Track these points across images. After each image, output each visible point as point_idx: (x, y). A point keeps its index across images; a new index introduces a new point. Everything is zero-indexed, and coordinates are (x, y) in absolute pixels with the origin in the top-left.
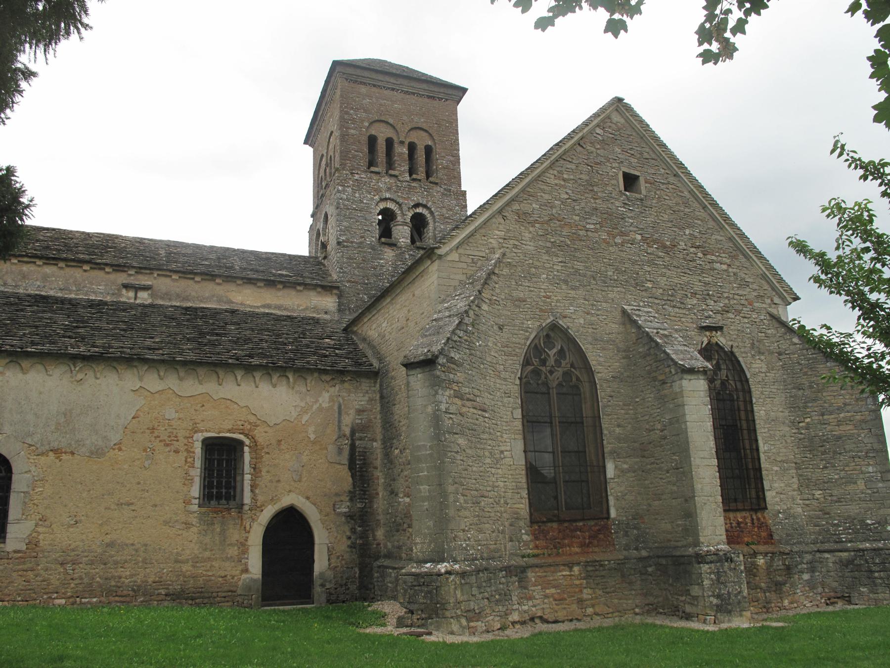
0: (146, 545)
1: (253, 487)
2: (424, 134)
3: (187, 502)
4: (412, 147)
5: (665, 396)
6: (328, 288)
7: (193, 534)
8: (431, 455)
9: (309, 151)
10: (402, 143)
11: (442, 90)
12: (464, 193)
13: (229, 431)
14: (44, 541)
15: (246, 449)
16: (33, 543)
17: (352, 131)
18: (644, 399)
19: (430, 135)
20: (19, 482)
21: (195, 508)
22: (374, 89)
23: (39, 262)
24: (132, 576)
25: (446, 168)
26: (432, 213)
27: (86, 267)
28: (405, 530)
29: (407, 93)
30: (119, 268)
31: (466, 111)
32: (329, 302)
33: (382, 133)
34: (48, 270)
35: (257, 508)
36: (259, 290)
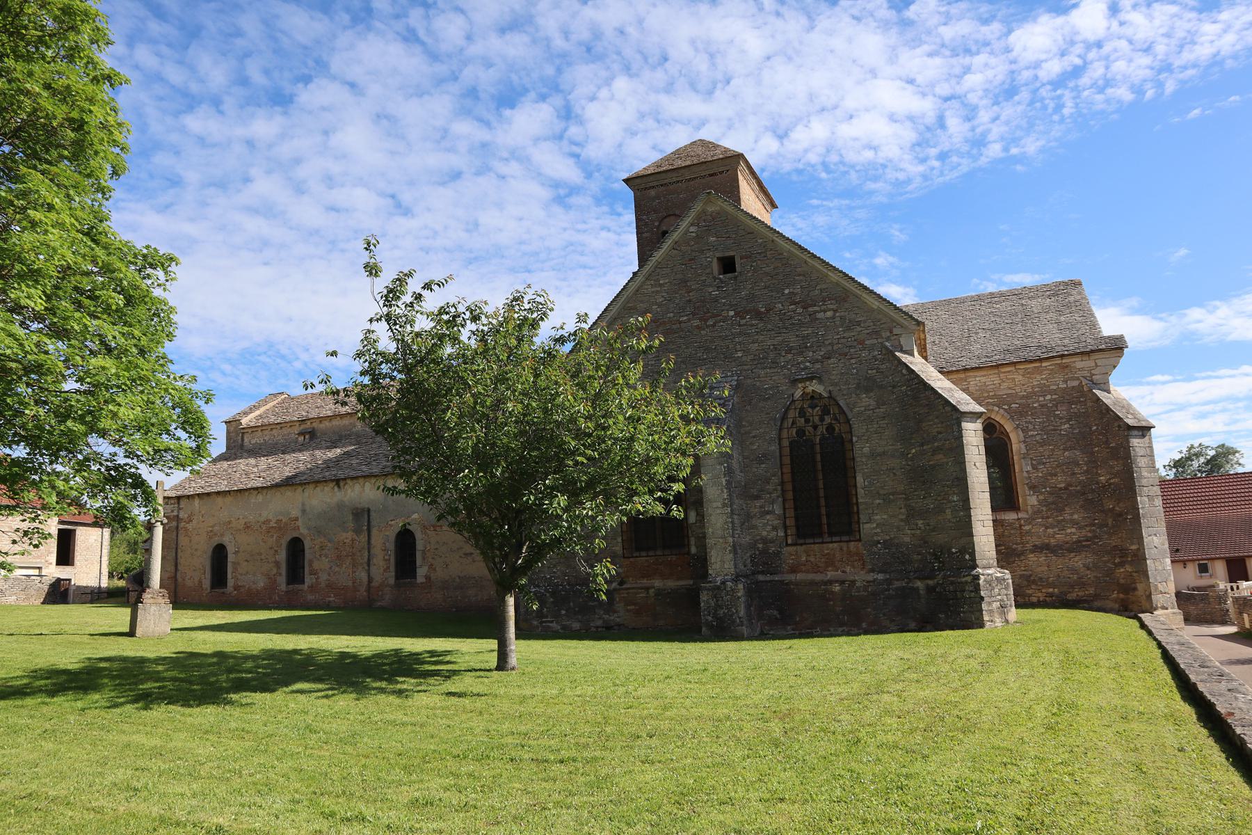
14: (433, 577)
16: (428, 578)
20: (420, 545)
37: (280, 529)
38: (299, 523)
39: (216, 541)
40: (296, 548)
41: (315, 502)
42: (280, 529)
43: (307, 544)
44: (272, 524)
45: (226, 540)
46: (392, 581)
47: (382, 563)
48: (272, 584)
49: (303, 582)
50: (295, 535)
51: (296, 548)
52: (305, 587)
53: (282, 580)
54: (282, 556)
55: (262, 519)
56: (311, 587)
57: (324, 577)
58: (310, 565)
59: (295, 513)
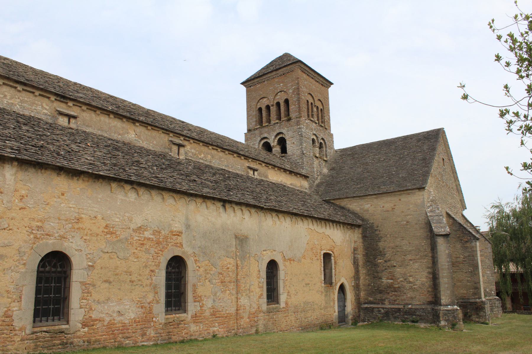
2: (320, 103)
3: (321, 283)
4: (317, 108)
5: (467, 247)
6: (306, 177)
7: (323, 297)
8: (448, 268)
9: (244, 89)
10: (315, 106)
11: (326, 82)
12: (332, 135)
15: (332, 258)
18: (455, 246)
19: (322, 104)
21: (323, 285)
22: (307, 77)
23: (219, 150)
24: (311, 316)
25: (327, 121)
26: (325, 143)
27: (235, 155)
28: (389, 293)
29: (316, 81)
30: (246, 157)
33: (311, 100)
34: (221, 154)
35: (336, 284)
37: (158, 243)
38: (183, 239)
40: (177, 267)
41: (199, 218)
42: (158, 243)
44: (147, 234)
45: (69, 247)
46: (264, 307)
47: (258, 290)
48: (147, 319)
49: (185, 311)
51: (177, 267)
52: (188, 316)
53: (160, 307)
55: (133, 226)
56: (195, 316)
57: (209, 303)
58: (194, 291)
59: (177, 226)
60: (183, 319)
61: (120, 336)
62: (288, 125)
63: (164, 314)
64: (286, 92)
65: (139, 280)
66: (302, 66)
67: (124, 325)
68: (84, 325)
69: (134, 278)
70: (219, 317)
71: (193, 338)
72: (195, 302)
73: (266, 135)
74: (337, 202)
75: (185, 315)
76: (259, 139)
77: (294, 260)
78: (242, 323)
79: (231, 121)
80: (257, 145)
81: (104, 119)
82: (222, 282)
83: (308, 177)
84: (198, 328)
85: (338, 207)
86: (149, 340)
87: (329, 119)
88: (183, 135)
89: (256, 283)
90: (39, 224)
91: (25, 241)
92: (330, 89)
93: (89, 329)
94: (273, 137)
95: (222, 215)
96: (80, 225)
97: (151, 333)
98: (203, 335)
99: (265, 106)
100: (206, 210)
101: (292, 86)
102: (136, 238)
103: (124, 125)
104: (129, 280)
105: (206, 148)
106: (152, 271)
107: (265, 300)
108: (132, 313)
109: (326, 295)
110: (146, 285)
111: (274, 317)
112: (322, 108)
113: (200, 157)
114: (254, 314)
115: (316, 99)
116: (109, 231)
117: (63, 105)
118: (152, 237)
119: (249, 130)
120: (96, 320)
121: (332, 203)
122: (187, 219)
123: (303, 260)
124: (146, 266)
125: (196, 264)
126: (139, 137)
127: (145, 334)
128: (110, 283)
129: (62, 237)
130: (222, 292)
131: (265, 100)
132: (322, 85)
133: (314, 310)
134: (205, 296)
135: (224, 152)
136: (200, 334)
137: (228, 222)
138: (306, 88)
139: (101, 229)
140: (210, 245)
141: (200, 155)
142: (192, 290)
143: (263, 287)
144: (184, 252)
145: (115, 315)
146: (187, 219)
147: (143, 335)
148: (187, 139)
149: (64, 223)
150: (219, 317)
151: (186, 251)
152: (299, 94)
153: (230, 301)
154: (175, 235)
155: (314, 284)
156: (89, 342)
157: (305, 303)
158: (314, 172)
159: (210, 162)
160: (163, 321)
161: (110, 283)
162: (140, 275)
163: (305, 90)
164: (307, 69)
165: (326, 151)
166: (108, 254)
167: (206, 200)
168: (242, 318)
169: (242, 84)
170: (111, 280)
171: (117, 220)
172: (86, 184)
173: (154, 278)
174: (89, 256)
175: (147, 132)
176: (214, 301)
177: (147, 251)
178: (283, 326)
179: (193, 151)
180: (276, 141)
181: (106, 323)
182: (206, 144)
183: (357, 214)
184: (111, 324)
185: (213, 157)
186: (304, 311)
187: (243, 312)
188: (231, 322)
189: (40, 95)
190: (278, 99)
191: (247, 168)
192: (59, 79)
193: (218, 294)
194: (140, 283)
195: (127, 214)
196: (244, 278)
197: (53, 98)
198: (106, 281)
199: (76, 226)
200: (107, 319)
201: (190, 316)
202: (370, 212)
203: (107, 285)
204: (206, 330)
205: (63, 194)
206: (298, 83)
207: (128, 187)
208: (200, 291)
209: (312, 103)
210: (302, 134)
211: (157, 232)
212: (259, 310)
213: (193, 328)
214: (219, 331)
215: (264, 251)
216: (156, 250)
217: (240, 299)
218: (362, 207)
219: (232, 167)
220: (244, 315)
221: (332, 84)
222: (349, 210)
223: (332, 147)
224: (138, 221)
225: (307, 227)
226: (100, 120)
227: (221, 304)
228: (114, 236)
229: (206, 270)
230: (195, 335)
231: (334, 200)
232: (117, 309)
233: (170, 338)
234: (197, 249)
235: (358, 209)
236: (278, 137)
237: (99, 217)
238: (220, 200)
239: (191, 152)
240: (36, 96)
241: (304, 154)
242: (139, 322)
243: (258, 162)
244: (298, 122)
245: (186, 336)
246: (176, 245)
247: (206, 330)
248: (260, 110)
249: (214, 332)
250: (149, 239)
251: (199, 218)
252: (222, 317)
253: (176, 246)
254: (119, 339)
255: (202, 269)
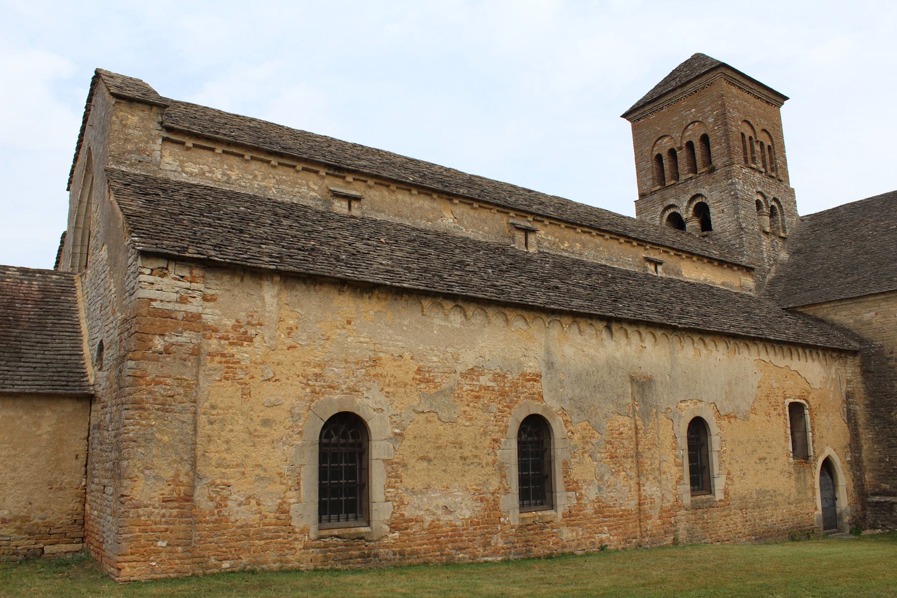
0: (775, 491)
1: (813, 442)
3: (788, 456)
4: (762, 144)
6: (748, 270)
7: (793, 482)
9: (627, 125)
10: (757, 142)
12: (792, 191)
13: (799, 398)
15: (806, 412)
17: (734, 128)
19: (770, 136)
24: (772, 516)
25: (781, 167)
26: (780, 206)
27: (622, 240)
29: (755, 96)
30: (641, 242)
31: (789, 115)
32: (748, 281)
33: (748, 133)
34: (598, 240)
35: (816, 459)
36: (714, 268)
37: (503, 394)
38: (544, 387)
39: (336, 403)
40: (535, 433)
41: (569, 351)
42: (503, 394)
43: (558, 428)
44: (484, 381)
46: (687, 499)
47: (674, 470)
48: (490, 518)
49: (552, 506)
50: (535, 408)
51: (535, 433)
52: (557, 515)
53: (510, 501)
54: (510, 452)
55: (460, 368)
56: (569, 515)
57: (591, 493)
58: (566, 473)
59: (532, 365)
60: (549, 519)
61: (450, 545)
62: (711, 180)
63: (517, 511)
64: (705, 122)
65: (476, 456)
66: (729, 73)
67: (455, 529)
68: (394, 528)
69: (467, 453)
70: (609, 516)
71: (567, 550)
72: (568, 490)
73: (672, 201)
74: (810, 311)
75: (552, 512)
76: (661, 209)
77: (736, 417)
78: (649, 527)
79: (611, 181)
80: (658, 219)
81: (403, 198)
82: (612, 458)
83: (753, 269)
84: (574, 534)
85: (813, 320)
86: (495, 553)
87: (785, 163)
88: (531, 213)
89: (671, 458)
90: (317, 370)
91: (300, 398)
92: (781, 109)
93: (401, 535)
94: (685, 204)
95: (606, 343)
96: (378, 370)
97: (498, 541)
98: (584, 547)
99: (666, 151)
100: (579, 336)
101: (712, 111)
102: (468, 387)
103: (435, 205)
104: (458, 457)
105: (572, 232)
106: (495, 441)
107: (688, 487)
108: (466, 510)
109: (798, 479)
110: (487, 464)
111: (705, 516)
112: (770, 144)
113: (562, 247)
114: (669, 510)
115: (758, 129)
116: (424, 377)
117: (339, 182)
118: (492, 384)
119: (642, 195)
120: (411, 520)
121: (801, 313)
122: (548, 352)
123: (752, 416)
124: (485, 433)
125: (566, 427)
126: (460, 222)
127: (489, 544)
128: (430, 460)
129: (353, 390)
130: (613, 474)
131: (666, 140)
132: (767, 102)
133: (777, 504)
134: (584, 481)
135: (603, 236)
136: (578, 545)
137: (618, 355)
138: (738, 111)
139: (411, 375)
140: (588, 395)
141: (563, 244)
142: (561, 471)
143: (682, 466)
144: (545, 409)
145: (439, 512)
146: (548, 352)
147: (486, 544)
148: (539, 218)
149: (353, 367)
150: (609, 516)
151: (549, 405)
152: (726, 124)
153: (627, 489)
154: (529, 380)
155: (775, 459)
156: (402, 554)
157: (758, 492)
158: (763, 259)
159: (580, 254)
160: (517, 523)
161: (430, 460)
162: (476, 448)
163: (736, 114)
164: (737, 77)
165: (783, 220)
166: (425, 415)
167: (578, 319)
168: (649, 517)
169: (624, 116)
170: (431, 456)
171: (435, 359)
172: (384, 303)
173: (499, 452)
174: (395, 419)
175: (472, 212)
176: (600, 489)
177: (486, 409)
178: (721, 532)
179: (550, 238)
180: (691, 209)
181: (426, 525)
182: (572, 224)
183: (849, 330)
184: (434, 528)
185: (584, 245)
186: (757, 506)
187: (651, 508)
188: (631, 525)
189: (304, 169)
190: (690, 135)
191: (643, 261)
192: (329, 141)
193: (606, 478)
194: (476, 460)
195: (450, 350)
196: (649, 449)
197: (323, 172)
198: (423, 458)
199: (373, 372)
200: (428, 519)
201: (560, 515)
202: (874, 326)
203: (425, 464)
204: (589, 538)
205: (349, 323)
206: (723, 105)
207: (448, 305)
208: (576, 472)
209: (750, 138)
210: (736, 194)
211: (499, 377)
212: (678, 505)
213: (567, 534)
214: (609, 540)
215: (681, 402)
216: (500, 407)
217: (644, 485)
218: (858, 318)
219: (618, 261)
220: (652, 512)
221: (786, 98)
222: (833, 325)
223: (794, 213)
224: (469, 359)
225: (757, 358)
226: (397, 200)
227: (612, 494)
228: (432, 385)
229: (583, 437)
230: (571, 546)
231: (803, 307)
232: (442, 502)
233: (530, 551)
234: (568, 403)
235: (851, 321)
236: (695, 203)
237: (407, 355)
238: (601, 318)
239: (547, 239)
240: (298, 171)
241: (742, 229)
242: (478, 524)
243: (662, 249)
244: (728, 172)
245: (555, 547)
246: (532, 396)
247: (589, 538)
248: (659, 158)
249: (601, 541)
250: (487, 388)
251: (569, 351)
252: (615, 516)
253: (533, 399)
254: (447, 551)
255: (577, 436)
